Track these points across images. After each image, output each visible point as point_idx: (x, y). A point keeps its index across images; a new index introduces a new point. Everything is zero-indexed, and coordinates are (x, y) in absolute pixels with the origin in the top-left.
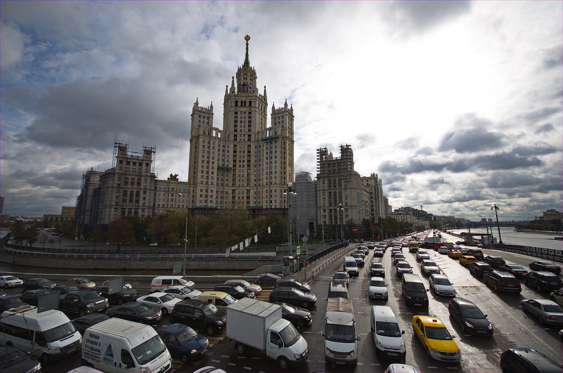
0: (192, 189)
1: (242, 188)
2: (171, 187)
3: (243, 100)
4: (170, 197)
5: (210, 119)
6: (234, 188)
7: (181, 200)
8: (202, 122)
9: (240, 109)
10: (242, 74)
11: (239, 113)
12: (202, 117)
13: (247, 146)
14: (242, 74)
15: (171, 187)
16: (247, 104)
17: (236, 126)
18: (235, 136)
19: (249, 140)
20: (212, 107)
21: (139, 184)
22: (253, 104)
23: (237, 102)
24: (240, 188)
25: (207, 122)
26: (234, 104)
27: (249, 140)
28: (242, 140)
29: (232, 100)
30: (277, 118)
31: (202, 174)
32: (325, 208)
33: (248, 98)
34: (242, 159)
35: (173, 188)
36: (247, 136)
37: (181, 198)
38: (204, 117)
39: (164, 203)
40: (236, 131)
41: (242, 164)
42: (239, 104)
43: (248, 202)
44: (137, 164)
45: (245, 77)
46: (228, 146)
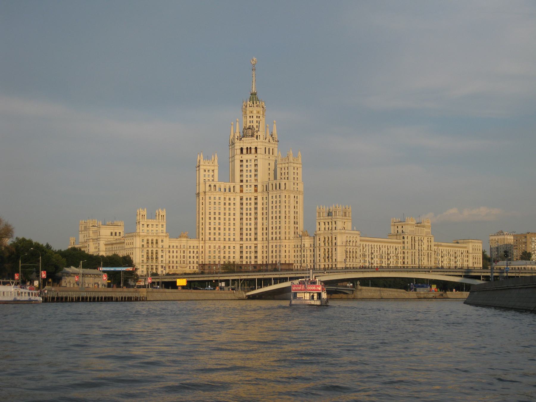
0: (201, 245)
1: (250, 242)
2: (182, 244)
3: (249, 148)
4: (182, 254)
6: (241, 242)
7: (192, 257)
8: (207, 176)
9: (245, 157)
10: (248, 112)
11: (245, 161)
13: (253, 198)
15: (182, 244)
16: (253, 151)
19: (256, 191)
21: (157, 243)
22: (258, 150)
23: (242, 149)
24: (247, 242)
25: (212, 176)
26: (239, 151)
27: (256, 191)
30: (283, 169)
31: (210, 231)
32: (319, 264)
33: (253, 144)
34: (249, 212)
36: (253, 186)
37: (192, 255)
39: (177, 259)
40: (242, 181)
41: (249, 217)
42: (245, 151)
43: (256, 257)
45: (251, 115)
46: (234, 199)
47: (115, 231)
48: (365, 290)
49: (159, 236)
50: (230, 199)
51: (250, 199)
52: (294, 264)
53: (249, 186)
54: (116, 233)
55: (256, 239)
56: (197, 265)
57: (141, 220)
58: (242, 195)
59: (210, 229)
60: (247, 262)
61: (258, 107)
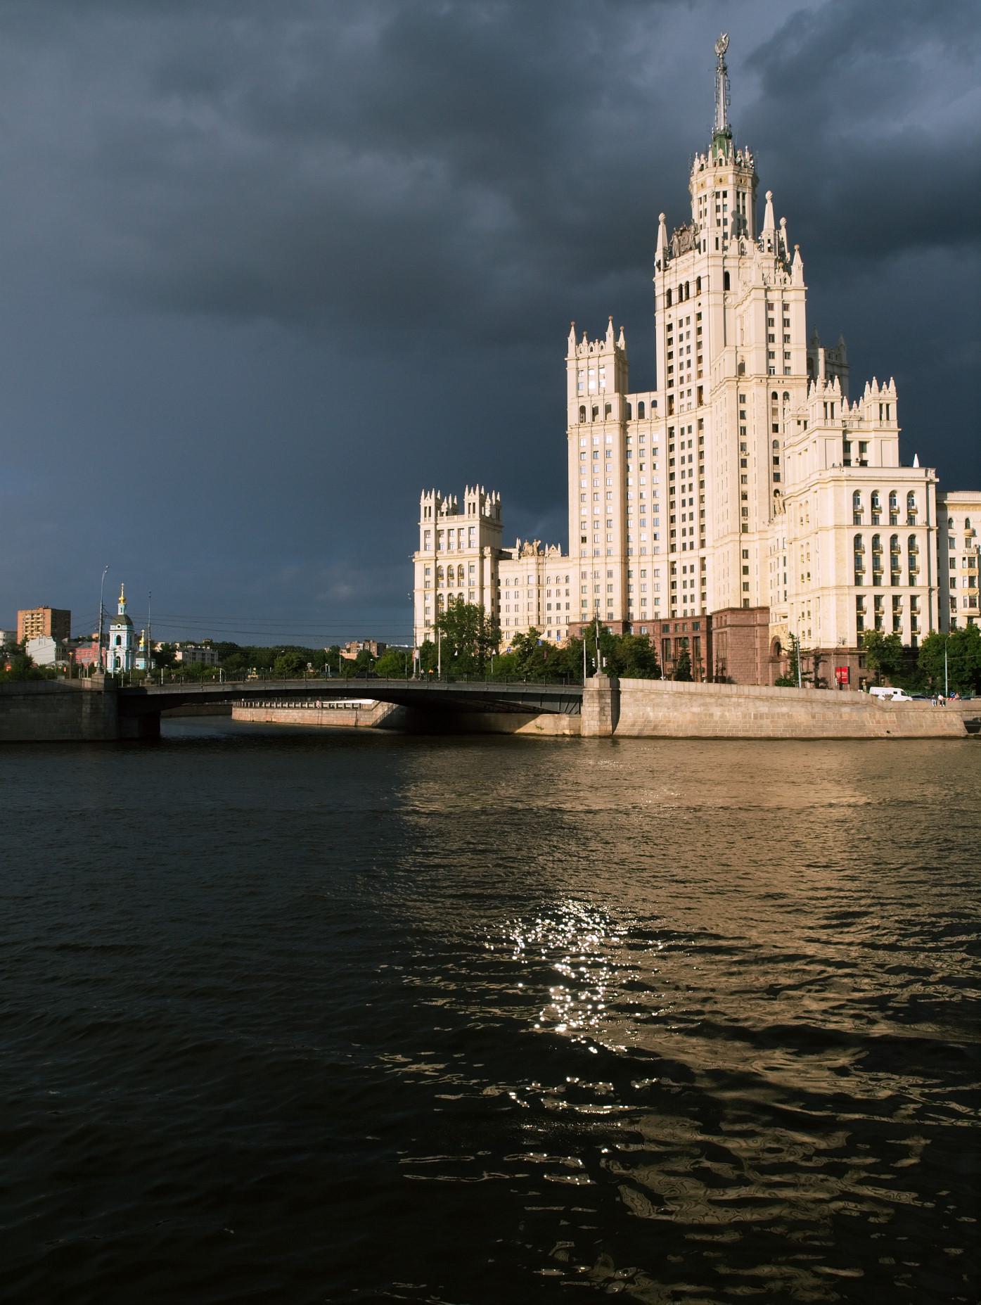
6: (673, 557)
15: (525, 574)
18: (671, 398)
21: (461, 575)
22: (704, 283)
27: (700, 402)
28: (685, 408)
33: (691, 271)
36: (694, 392)
43: (703, 596)
44: (455, 533)
45: (701, 195)
48: (633, 692)
52: (771, 611)
53: (686, 393)
56: (567, 627)
58: (672, 421)
60: (685, 612)
61: (721, 165)
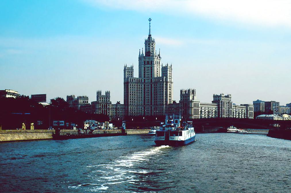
0: (126, 107)
2: (118, 107)
5: (133, 72)
9: (146, 66)
11: (146, 68)
12: (129, 72)
14: (147, 44)
16: (150, 63)
17: (145, 75)
20: (133, 66)
22: (153, 63)
23: (145, 62)
24: (147, 106)
26: (143, 63)
29: (143, 61)
35: (119, 108)
36: (150, 80)
38: (130, 72)
42: (146, 63)
45: (149, 46)
47: (85, 100)
49: (107, 103)
50: (139, 86)
51: (149, 86)
54: (85, 101)
55: (151, 104)
57: (99, 95)
59: (131, 99)
